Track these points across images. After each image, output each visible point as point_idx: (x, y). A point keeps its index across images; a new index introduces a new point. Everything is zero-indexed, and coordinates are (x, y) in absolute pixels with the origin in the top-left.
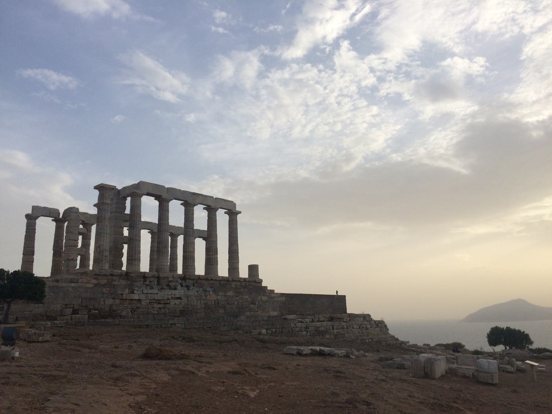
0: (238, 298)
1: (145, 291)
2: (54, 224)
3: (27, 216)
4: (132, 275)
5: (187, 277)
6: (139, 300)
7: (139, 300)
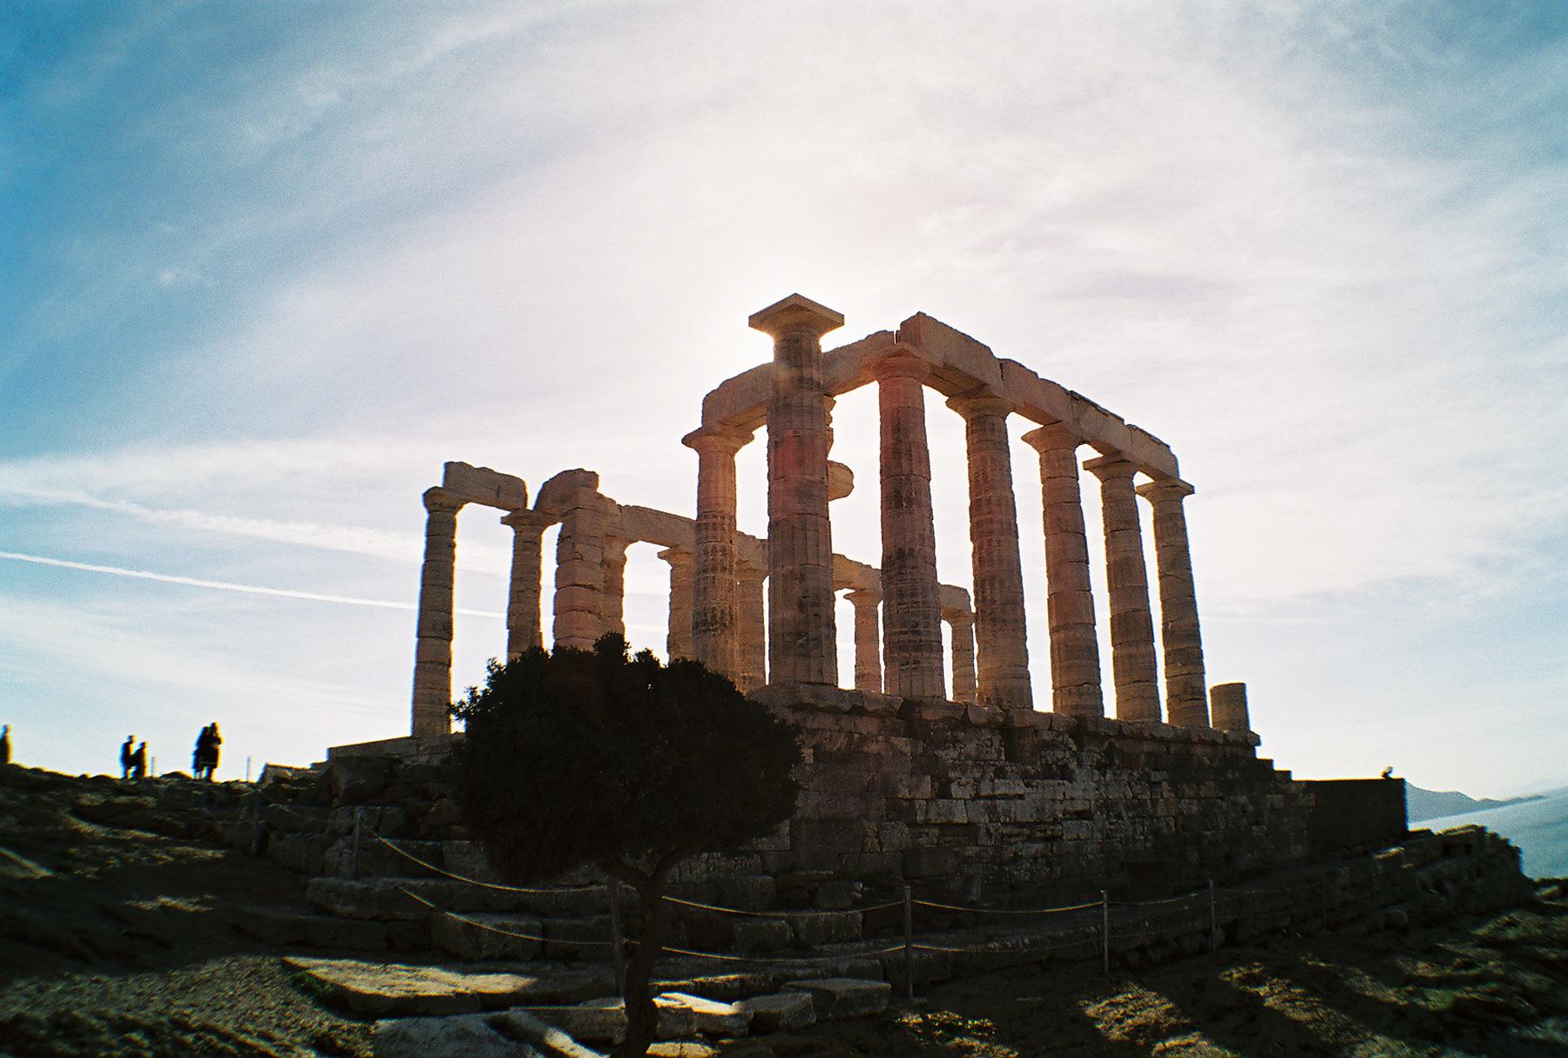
0: (1224, 805)
1: (985, 790)
2: (509, 532)
3: (431, 497)
4: (928, 715)
5: (1091, 728)
6: (970, 826)
7: (969, 823)
